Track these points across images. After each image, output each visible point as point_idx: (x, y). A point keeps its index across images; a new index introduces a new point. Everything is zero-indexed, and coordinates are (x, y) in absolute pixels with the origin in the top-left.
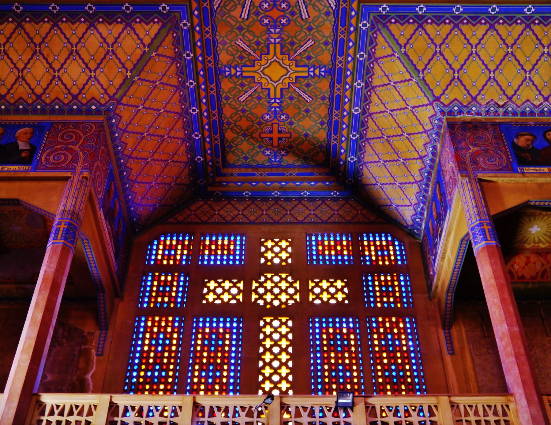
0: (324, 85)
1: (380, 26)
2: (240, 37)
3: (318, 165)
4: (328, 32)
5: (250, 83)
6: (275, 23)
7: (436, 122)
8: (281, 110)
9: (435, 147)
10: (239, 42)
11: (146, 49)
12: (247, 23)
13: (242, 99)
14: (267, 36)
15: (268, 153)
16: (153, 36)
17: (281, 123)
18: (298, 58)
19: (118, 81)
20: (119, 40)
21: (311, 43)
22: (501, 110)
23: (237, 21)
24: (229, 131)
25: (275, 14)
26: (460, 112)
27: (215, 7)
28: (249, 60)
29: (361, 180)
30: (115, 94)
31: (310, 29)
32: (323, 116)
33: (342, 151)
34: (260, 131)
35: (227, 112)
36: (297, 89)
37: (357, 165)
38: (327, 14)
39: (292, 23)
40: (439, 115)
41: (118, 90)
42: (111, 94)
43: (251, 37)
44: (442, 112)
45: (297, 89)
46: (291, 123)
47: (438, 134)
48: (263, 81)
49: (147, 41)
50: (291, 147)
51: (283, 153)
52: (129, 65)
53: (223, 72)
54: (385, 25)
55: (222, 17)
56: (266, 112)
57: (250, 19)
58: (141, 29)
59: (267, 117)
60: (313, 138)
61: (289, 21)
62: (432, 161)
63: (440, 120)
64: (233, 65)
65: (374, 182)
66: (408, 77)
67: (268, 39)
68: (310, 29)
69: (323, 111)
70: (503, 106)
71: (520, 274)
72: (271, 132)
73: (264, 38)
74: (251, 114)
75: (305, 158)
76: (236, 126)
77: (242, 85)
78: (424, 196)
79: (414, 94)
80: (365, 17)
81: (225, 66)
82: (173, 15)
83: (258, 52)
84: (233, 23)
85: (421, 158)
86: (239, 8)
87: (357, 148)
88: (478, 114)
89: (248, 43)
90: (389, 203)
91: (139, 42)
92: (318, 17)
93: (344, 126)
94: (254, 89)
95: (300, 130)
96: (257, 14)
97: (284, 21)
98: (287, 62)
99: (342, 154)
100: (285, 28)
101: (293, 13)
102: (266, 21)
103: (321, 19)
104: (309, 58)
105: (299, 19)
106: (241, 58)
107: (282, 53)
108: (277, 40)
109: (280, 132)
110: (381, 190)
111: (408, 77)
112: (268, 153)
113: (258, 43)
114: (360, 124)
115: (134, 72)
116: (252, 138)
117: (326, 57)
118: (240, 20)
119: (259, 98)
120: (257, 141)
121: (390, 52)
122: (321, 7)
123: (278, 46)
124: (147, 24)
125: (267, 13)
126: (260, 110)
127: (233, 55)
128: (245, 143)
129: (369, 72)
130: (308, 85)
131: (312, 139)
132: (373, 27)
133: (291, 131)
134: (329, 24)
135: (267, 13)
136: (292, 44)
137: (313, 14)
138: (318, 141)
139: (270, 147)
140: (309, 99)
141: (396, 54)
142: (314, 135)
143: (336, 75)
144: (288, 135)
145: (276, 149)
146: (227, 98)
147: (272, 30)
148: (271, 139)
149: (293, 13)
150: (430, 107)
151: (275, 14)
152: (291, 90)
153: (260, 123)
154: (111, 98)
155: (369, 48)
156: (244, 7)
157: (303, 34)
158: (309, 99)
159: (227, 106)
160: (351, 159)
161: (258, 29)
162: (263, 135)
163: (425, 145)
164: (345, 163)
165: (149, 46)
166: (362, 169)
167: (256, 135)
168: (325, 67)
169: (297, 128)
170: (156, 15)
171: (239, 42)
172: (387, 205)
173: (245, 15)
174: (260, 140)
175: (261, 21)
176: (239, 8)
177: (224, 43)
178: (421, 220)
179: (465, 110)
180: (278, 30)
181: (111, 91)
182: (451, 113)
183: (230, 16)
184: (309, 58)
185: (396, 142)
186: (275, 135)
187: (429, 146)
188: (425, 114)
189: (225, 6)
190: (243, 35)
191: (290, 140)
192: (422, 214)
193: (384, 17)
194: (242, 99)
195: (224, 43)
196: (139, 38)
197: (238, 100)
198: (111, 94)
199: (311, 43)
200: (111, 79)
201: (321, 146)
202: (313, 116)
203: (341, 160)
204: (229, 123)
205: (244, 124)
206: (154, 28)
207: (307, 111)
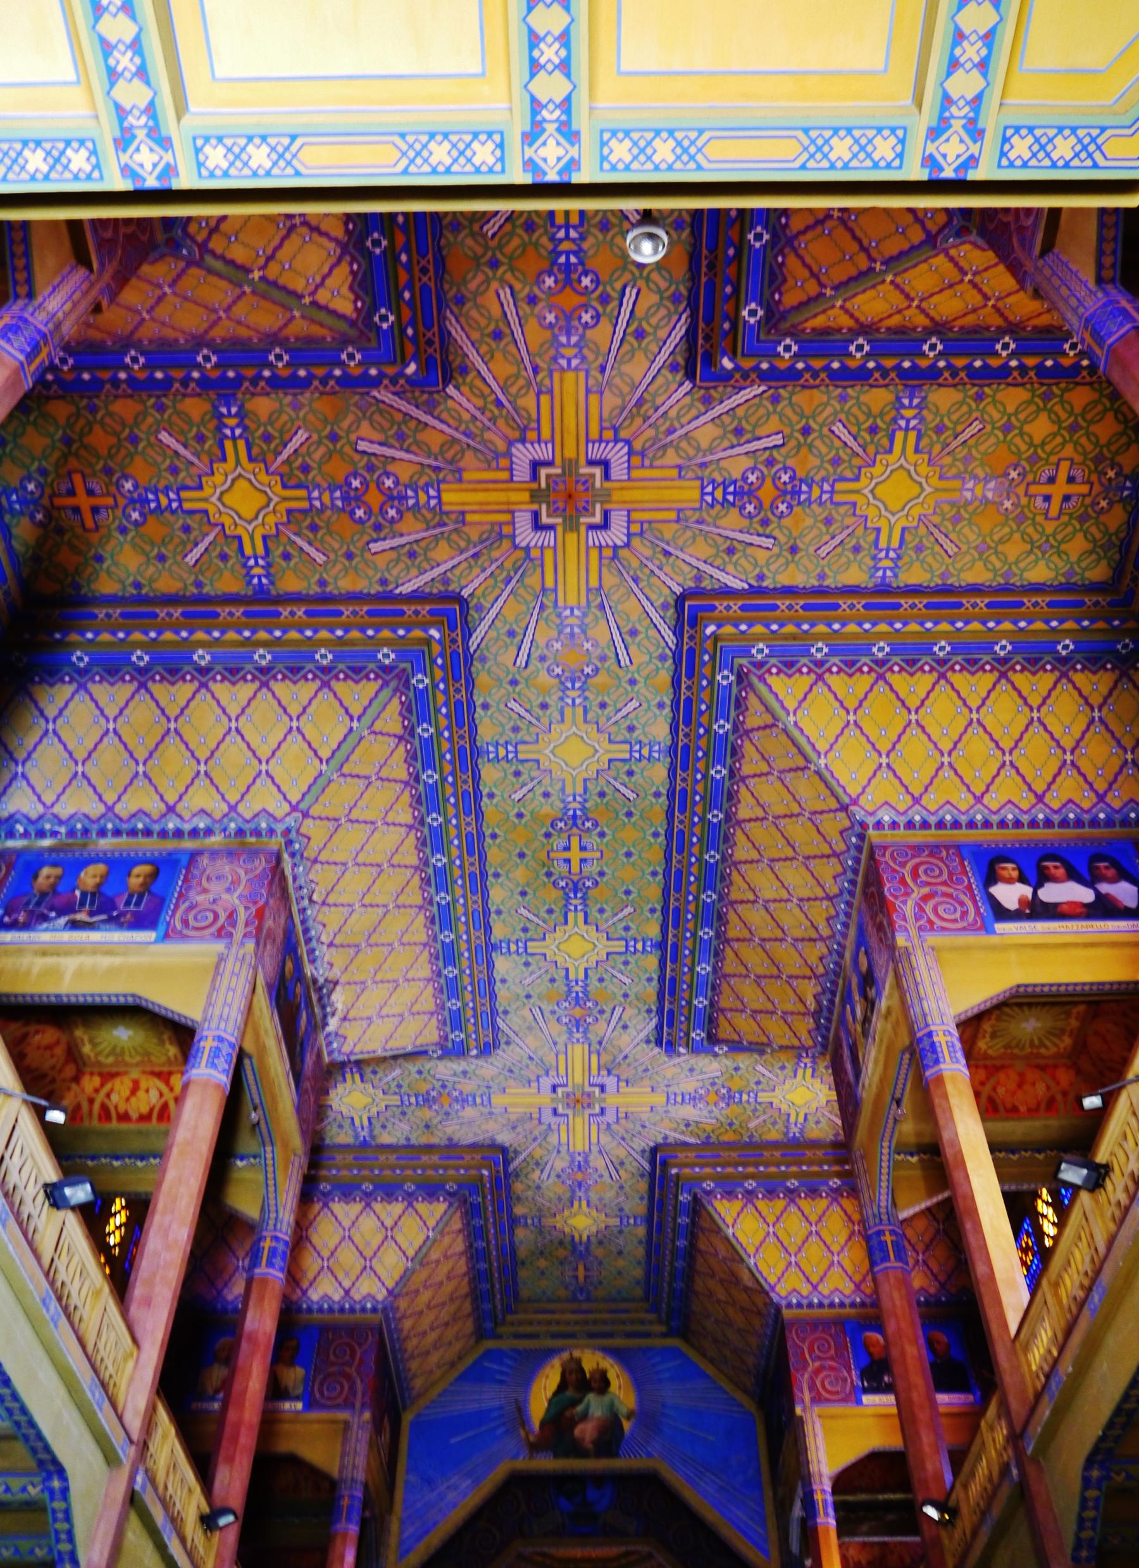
0: (228, 582)
1: (393, 684)
2: (315, 437)
3: (24, 584)
4: (345, 584)
5: (209, 453)
6: (352, 499)
7: (264, 825)
8: (152, 512)
9: (209, 832)
10: (302, 436)
11: (307, 300)
12: (348, 449)
13: (164, 436)
14: (325, 485)
15: (31, 487)
16: (332, 306)
17: (119, 512)
18: (284, 539)
19: (238, 253)
20: (315, 235)
21: (320, 558)
22: (306, 902)
23: (348, 432)
24: (73, 409)
25: (374, 498)
26: (293, 855)
27: (375, 393)
28: (263, 453)
29: (33, 682)
30: (213, 253)
31: (349, 556)
32: (156, 586)
33: (90, 635)
34: (87, 471)
35: (124, 408)
36: (210, 538)
37: (66, 669)
38: (383, 582)
39: (358, 527)
40: (279, 828)
41: (222, 258)
42: (211, 245)
43: (317, 455)
44: (287, 831)
45: (210, 538)
46: (123, 530)
47: (240, 832)
48: (218, 478)
49: (323, 296)
50: (60, 531)
51: (39, 517)
52: (273, 271)
53: (228, 401)
54: (396, 690)
55: (356, 405)
56: (143, 482)
57: (357, 457)
58: (341, 277)
59: (128, 485)
60: (96, 572)
61: (361, 521)
62: (178, 833)
63: (271, 832)
64: (247, 421)
65: (51, 712)
66: (325, 753)
67: (318, 486)
68: (349, 556)
69: (166, 584)
70: (311, 900)
71: (122, 1109)
72: (90, 493)
73: (318, 479)
74: (130, 456)
75: (36, 559)
76: (90, 425)
77: (201, 439)
78: (86, 832)
79: (295, 771)
80: (402, 655)
81: (241, 407)
82: (372, 335)
83: (285, 469)
84: (345, 424)
85: (171, 809)
86: (376, 436)
87: (112, 667)
88: (295, 879)
89: (304, 449)
90: (21, 755)
91: (318, 279)
92: (376, 568)
93: (153, 635)
94: (195, 460)
95: (109, 548)
96: (370, 468)
97: (360, 513)
98: (271, 520)
99: (83, 634)
100: (345, 518)
101: (378, 527)
102: (356, 483)
103: (371, 573)
104: (286, 556)
105: (366, 538)
106: (267, 438)
107: (289, 512)
108: (317, 504)
109: (95, 510)
110: (40, 733)
111: (325, 753)
112: (31, 487)
113: (305, 469)
114: (172, 666)
115: (263, 286)
116: (65, 456)
117: (290, 583)
118: (353, 437)
119: (174, 470)
120: (57, 465)
121: (356, 710)
122: (395, 572)
123: (305, 505)
124: (351, 288)
125: (372, 486)
126: (141, 472)
127: (270, 422)
128: (48, 441)
129: (294, 672)
130: (224, 557)
131: (89, 570)
132: (387, 669)
133: (103, 531)
134: (367, 584)
135: (372, 486)
136: (314, 528)
137: (381, 561)
138: (89, 581)
139: (48, 491)
140: (191, 559)
141: (355, 724)
142: (103, 574)
143: (262, 602)
144: (89, 523)
145: (45, 501)
146: (161, 408)
147: (338, 494)
148: (72, 493)
149: (378, 527)
150: (286, 808)
151: (374, 498)
152: (206, 528)
153: (108, 471)
154: (204, 247)
155: (341, 666)
156: (381, 444)
157: (336, 545)
158: (191, 559)
159: (138, 408)
160: (80, 658)
161: (338, 469)
162: (77, 479)
163: (203, 811)
164: (60, 642)
165: (314, 303)
166: (63, 681)
167: (73, 463)
168: (272, 583)
169: (112, 543)
170: (368, 300)
171: (302, 436)
172: (11, 754)
173: (362, 446)
174: (63, 471)
175: (355, 475)
176: (376, 436)
177: (296, 407)
178: (26, 835)
179: (297, 859)
180: (339, 503)
181: (216, 244)
182: (289, 843)
183: (358, 421)
184: (286, 556)
185: (173, 749)
186: (83, 501)
187: (208, 821)
188: (264, 800)
189: (381, 412)
190: (319, 443)
191: (79, 531)
192: (41, 834)
193: (407, 684)
194: (164, 436)
195: (296, 407)
196: (324, 278)
197: (168, 436)
198: (211, 245)
199: (320, 558)
200: (241, 236)
201: (77, 586)
202: (151, 570)
203: (65, 634)
204: (93, 409)
205: (99, 439)
206: (345, 305)
207: (161, 558)
